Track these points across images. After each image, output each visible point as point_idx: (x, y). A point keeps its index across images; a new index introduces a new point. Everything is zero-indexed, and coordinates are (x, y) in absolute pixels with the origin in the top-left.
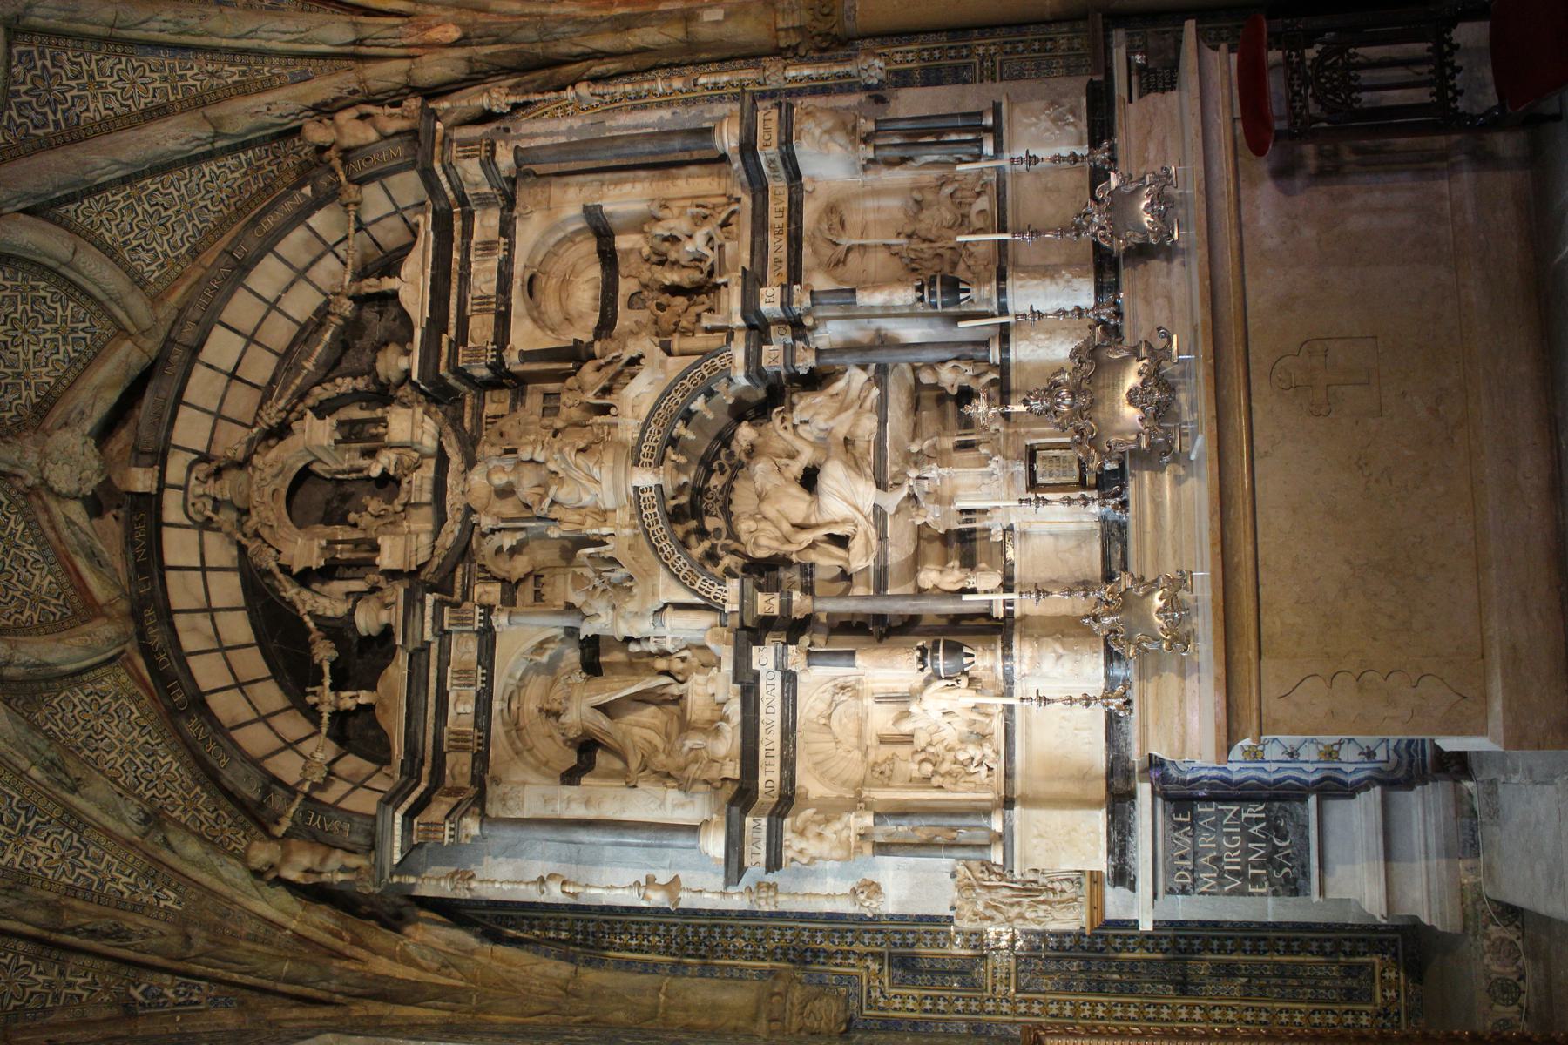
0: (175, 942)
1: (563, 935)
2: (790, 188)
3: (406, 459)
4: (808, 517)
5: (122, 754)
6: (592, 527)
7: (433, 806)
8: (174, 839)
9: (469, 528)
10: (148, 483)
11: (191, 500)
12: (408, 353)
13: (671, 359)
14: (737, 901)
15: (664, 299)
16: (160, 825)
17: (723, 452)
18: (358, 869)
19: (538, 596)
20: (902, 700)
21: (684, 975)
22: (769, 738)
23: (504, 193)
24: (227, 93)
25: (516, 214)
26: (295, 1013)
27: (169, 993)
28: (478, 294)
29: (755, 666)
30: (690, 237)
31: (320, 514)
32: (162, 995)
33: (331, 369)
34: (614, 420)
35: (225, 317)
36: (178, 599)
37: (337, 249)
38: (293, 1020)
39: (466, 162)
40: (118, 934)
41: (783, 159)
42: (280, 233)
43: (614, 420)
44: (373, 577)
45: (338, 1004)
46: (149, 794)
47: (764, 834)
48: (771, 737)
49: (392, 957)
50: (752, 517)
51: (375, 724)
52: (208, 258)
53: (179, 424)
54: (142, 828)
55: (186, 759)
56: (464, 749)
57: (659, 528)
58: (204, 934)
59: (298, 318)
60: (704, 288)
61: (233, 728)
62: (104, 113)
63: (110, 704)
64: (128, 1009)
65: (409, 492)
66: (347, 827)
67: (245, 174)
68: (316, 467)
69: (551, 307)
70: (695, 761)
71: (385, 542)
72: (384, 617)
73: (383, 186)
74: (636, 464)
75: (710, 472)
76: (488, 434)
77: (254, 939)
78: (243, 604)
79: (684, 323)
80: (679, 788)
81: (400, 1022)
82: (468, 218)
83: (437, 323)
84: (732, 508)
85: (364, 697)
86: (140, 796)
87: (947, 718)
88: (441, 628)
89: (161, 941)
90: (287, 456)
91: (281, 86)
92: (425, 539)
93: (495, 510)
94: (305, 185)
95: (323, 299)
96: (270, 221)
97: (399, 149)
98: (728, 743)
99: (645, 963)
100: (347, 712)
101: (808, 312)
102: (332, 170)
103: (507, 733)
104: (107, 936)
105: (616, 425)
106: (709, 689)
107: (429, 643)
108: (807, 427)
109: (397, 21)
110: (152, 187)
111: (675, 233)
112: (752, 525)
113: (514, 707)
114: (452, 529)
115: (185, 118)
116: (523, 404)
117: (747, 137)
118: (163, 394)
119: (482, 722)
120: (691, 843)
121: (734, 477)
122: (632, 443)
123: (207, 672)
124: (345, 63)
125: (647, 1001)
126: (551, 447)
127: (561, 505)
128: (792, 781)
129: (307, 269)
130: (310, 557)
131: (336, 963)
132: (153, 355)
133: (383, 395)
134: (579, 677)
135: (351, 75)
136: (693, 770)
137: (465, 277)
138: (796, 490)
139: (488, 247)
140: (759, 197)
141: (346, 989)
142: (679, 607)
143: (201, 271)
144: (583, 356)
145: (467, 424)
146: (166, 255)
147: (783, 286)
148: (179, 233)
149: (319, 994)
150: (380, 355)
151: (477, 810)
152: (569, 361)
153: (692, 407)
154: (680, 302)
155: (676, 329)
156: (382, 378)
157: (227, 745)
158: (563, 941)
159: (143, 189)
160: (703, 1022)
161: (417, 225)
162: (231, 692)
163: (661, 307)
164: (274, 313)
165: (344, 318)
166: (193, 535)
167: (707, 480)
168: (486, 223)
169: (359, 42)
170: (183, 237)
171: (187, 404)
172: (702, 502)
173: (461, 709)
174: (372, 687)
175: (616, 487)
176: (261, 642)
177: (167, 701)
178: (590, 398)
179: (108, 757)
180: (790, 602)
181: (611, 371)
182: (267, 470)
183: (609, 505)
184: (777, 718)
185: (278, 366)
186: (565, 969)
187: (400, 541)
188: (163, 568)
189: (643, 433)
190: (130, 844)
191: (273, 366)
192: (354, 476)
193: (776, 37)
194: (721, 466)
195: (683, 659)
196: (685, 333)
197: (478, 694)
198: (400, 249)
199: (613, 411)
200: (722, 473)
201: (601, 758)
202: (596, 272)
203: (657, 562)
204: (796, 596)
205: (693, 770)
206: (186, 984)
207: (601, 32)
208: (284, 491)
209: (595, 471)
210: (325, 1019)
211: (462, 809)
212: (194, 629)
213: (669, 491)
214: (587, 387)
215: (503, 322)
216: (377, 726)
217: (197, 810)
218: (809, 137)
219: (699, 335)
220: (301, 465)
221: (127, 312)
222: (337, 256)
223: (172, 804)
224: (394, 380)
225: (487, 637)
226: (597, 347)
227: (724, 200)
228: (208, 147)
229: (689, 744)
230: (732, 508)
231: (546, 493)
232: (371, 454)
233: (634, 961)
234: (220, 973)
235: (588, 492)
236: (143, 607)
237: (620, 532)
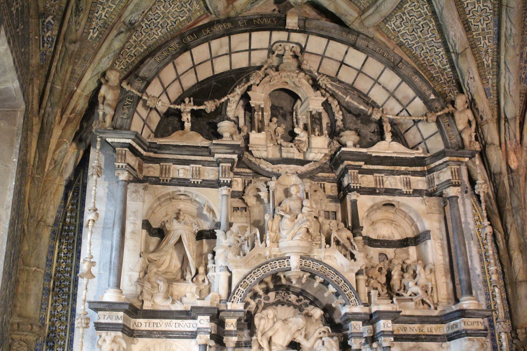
0: (73, 37)
1: (68, 220)
2: (443, 335)
3: (303, 145)
4: (275, 345)
5: (163, 13)
6: (270, 235)
7: (134, 158)
8: (122, 35)
9: (269, 175)
10: (290, 25)
11: (283, 44)
12: (355, 145)
13: (354, 275)
14: (81, 307)
15: (384, 271)
16: (129, 30)
17: (308, 301)
18: (104, 121)
19: (236, 209)
21: (45, 280)
22: (163, 325)
23: (435, 191)
24: (478, 59)
25: (425, 197)
26: (36, 91)
27: (49, 34)
28: (385, 179)
30: (416, 284)
31: (276, 104)
32: (48, 30)
33: (346, 109)
34: (323, 246)
35: (370, 59)
36: (235, 38)
37: (404, 111)
38: (33, 91)
39: (449, 173)
40: (78, 10)
41: (458, 332)
42: (411, 84)
43: (323, 246)
44: (245, 129)
45: (39, 111)
46: (143, 25)
47: (114, 321)
48: (163, 325)
49: (61, 137)
50: (275, 316)
51: (174, 130)
52: (398, 51)
53: (319, 38)
54: (127, 22)
55: (159, 42)
56: (161, 173)
57: (269, 269)
58: (76, 50)
59: (370, 93)
60: (390, 292)
61: (174, 63)
62: (465, 3)
63: (186, 7)
64: (42, 15)
65: (287, 147)
66: (125, 116)
67: (439, 68)
68: (299, 102)
69: (378, 215)
70: (153, 287)
71: (263, 135)
72: (226, 135)
73: (436, 133)
75: (298, 295)
76: (315, 185)
77: (73, 72)
78: (233, 68)
79: (372, 281)
80: (139, 279)
81: (29, 140)
82: (422, 174)
83: (370, 159)
84: (279, 306)
85: (188, 125)
86: (143, 21)
88: (220, 162)
89: (74, 30)
90: (304, 89)
91: (483, 84)
92: (264, 154)
93: (278, 188)
94: (435, 95)
95: (380, 105)
96: (417, 80)
97: (455, 140)
98: (161, 303)
99: (51, 261)
100: (181, 117)
101: (380, 345)
102: (443, 108)
103: (169, 194)
104: (77, 6)
105: (321, 248)
106: (188, 294)
107: (213, 156)
108: (321, 344)
109: (518, 138)
110: (431, 25)
111: (418, 276)
112: (271, 316)
113: (182, 197)
114: (269, 167)
115: (465, 39)
116: (330, 202)
117: (469, 313)
118: (333, 31)
119: (175, 181)
120: (111, 284)
121: (295, 307)
122: (312, 255)
123: (201, 52)
124: (496, 113)
125: (33, 261)
126: (310, 215)
127: (281, 220)
128: (140, 336)
129: (394, 97)
130: (255, 100)
131: (59, 110)
132: (351, 27)
133: (334, 133)
134: (196, 229)
135: (490, 116)
136: (148, 286)
137: (392, 173)
138: (289, 339)
139: (408, 184)
140: (438, 320)
141: (46, 115)
143: (392, 48)
144: (355, 231)
145: (320, 174)
146: (399, 32)
147: (392, 332)
148: (410, 37)
149: (44, 103)
150: (354, 132)
151: (131, 179)
152: (352, 224)
153: (330, 286)
154: (383, 280)
155: (370, 277)
156: (342, 134)
157: (167, 60)
158: (65, 220)
159: (430, 21)
160: (20, 289)
161: (417, 149)
162: (191, 63)
163: (380, 270)
164: (373, 82)
165: (371, 115)
166: (266, 45)
167: (294, 293)
168: (420, 182)
169: (506, 120)
170: (408, 39)
171: (328, 42)
173: (181, 171)
174: (192, 129)
175: (289, 247)
176: (214, 76)
177: (187, 33)
178: (334, 235)
179: (161, 7)
180: (232, 335)
181: (348, 245)
182: (297, 79)
183: (281, 244)
184: (173, 328)
185: (347, 84)
186: (51, 221)
187: (263, 142)
188: (250, 31)
189: (317, 261)
190: (120, 17)
191: (347, 82)
192: (295, 120)
193: (522, 328)
194: (301, 300)
195: (204, 281)
196: (367, 281)
197: (188, 180)
198: (405, 141)
199: (328, 246)
200: (297, 301)
201: (155, 240)
202: (397, 237)
203: (252, 268)
204: (235, 339)
205: (148, 286)
206: (53, 41)
207: (519, 239)
208: (287, 87)
209: (297, 237)
210: (32, 105)
211: (132, 171)
212: (221, 46)
213: (288, 274)
214: (340, 233)
215: (372, 192)
216: (174, 131)
217: (136, 47)
218: (470, 345)
219: (367, 289)
220: (300, 95)
221: (371, 14)
222: (401, 111)
223: (139, 36)
224: (341, 139)
225: (216, 184)
226: (359, 238)
227: (436, 301)
228: (451, 50)
229: (161, 284)
230: (279, 306)
231: (287, 213)
232: (305, 128)
233: (53, 255)
234: (57, 57)
235: (287, 234)
236: (232, 24)
237: (267, 250)
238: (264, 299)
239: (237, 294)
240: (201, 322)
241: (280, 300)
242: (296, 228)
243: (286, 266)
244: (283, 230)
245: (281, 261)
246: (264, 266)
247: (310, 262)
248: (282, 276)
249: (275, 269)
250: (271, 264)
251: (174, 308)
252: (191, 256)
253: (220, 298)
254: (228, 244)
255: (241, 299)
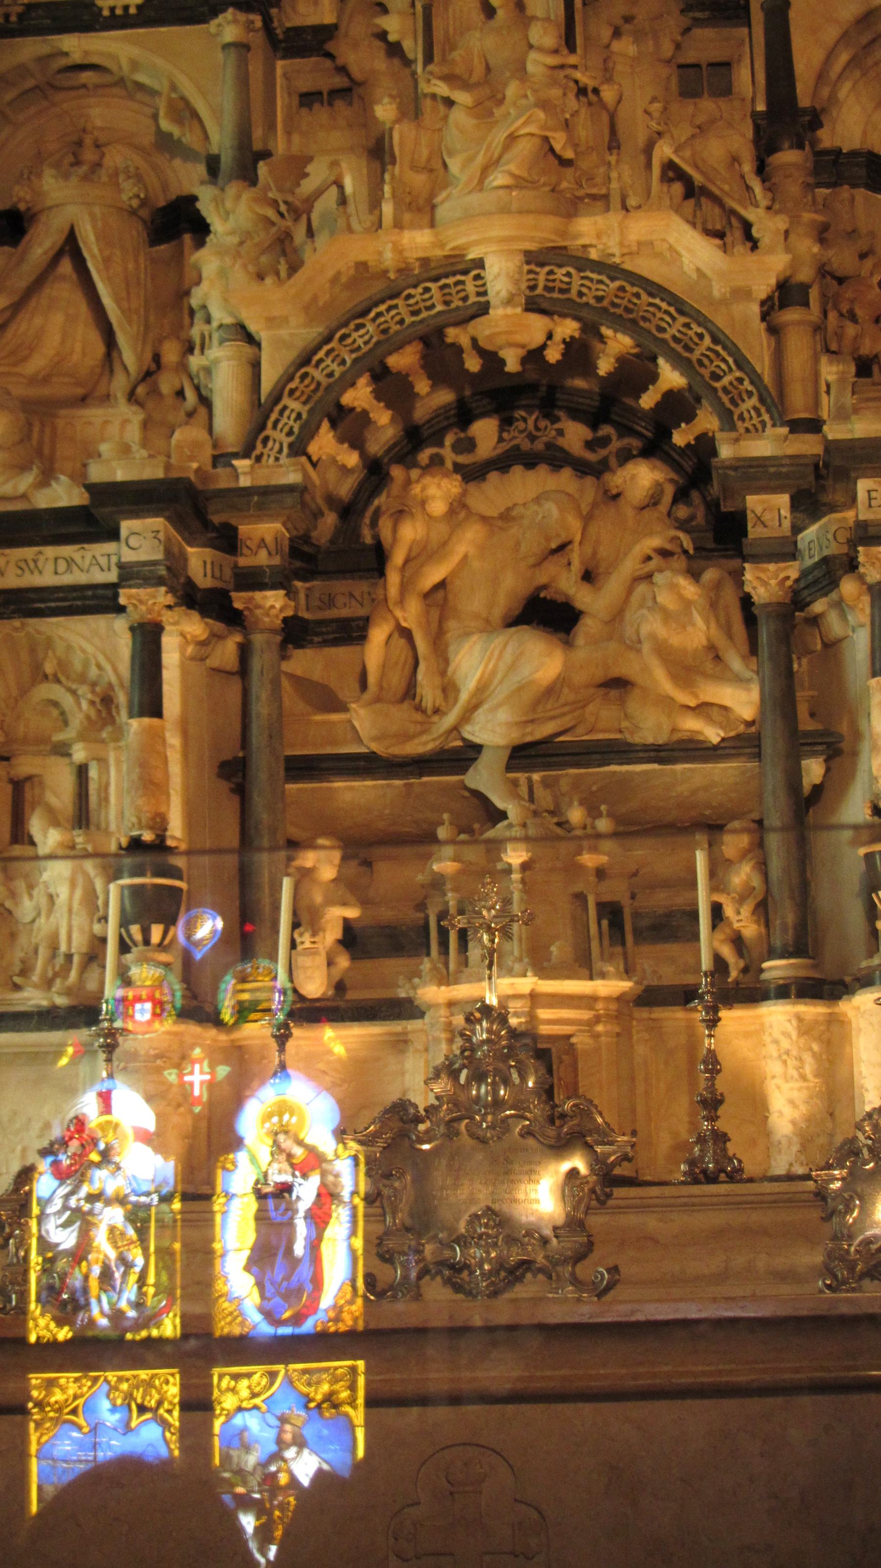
13: (755, 309)
19: (308, 99)
20: (82, 816)
29: (126, 526)
34: (615, 201)
43: (615, 201)
74: (530, 257)
75: (594, 420)
84: (517, 471)
87: (44, 901)
103: (22, 70)
113: (86, 77)
121: (582, 468)
126: (554, 82)
142: (256, 366)
153: (661, 361)
167: (575, 414)
172: (529, 408)
180: (262, 586)
181: (723, 186)
184: (47, 579)
189: (599, 266)
194: (605, 442)
200: (590, 445)
209: (499, 179)
213: (483, 329)
226: (788, 157)
238: (458, 448)
239: (275, 426)
240: (133, 542)
241: (517, 448)
242: (500, 136)
243: (473, 299)
244: (451, 154)
245: (451, 281)
246: (382, 308)
247: (568, 274)
248: (464, 341)
249: (424, 314)
250: (409, 296)
251: (44, 500)
252: (117, 301)
253: (215, 446)
254: (235, 240)
255: (291, 445)
